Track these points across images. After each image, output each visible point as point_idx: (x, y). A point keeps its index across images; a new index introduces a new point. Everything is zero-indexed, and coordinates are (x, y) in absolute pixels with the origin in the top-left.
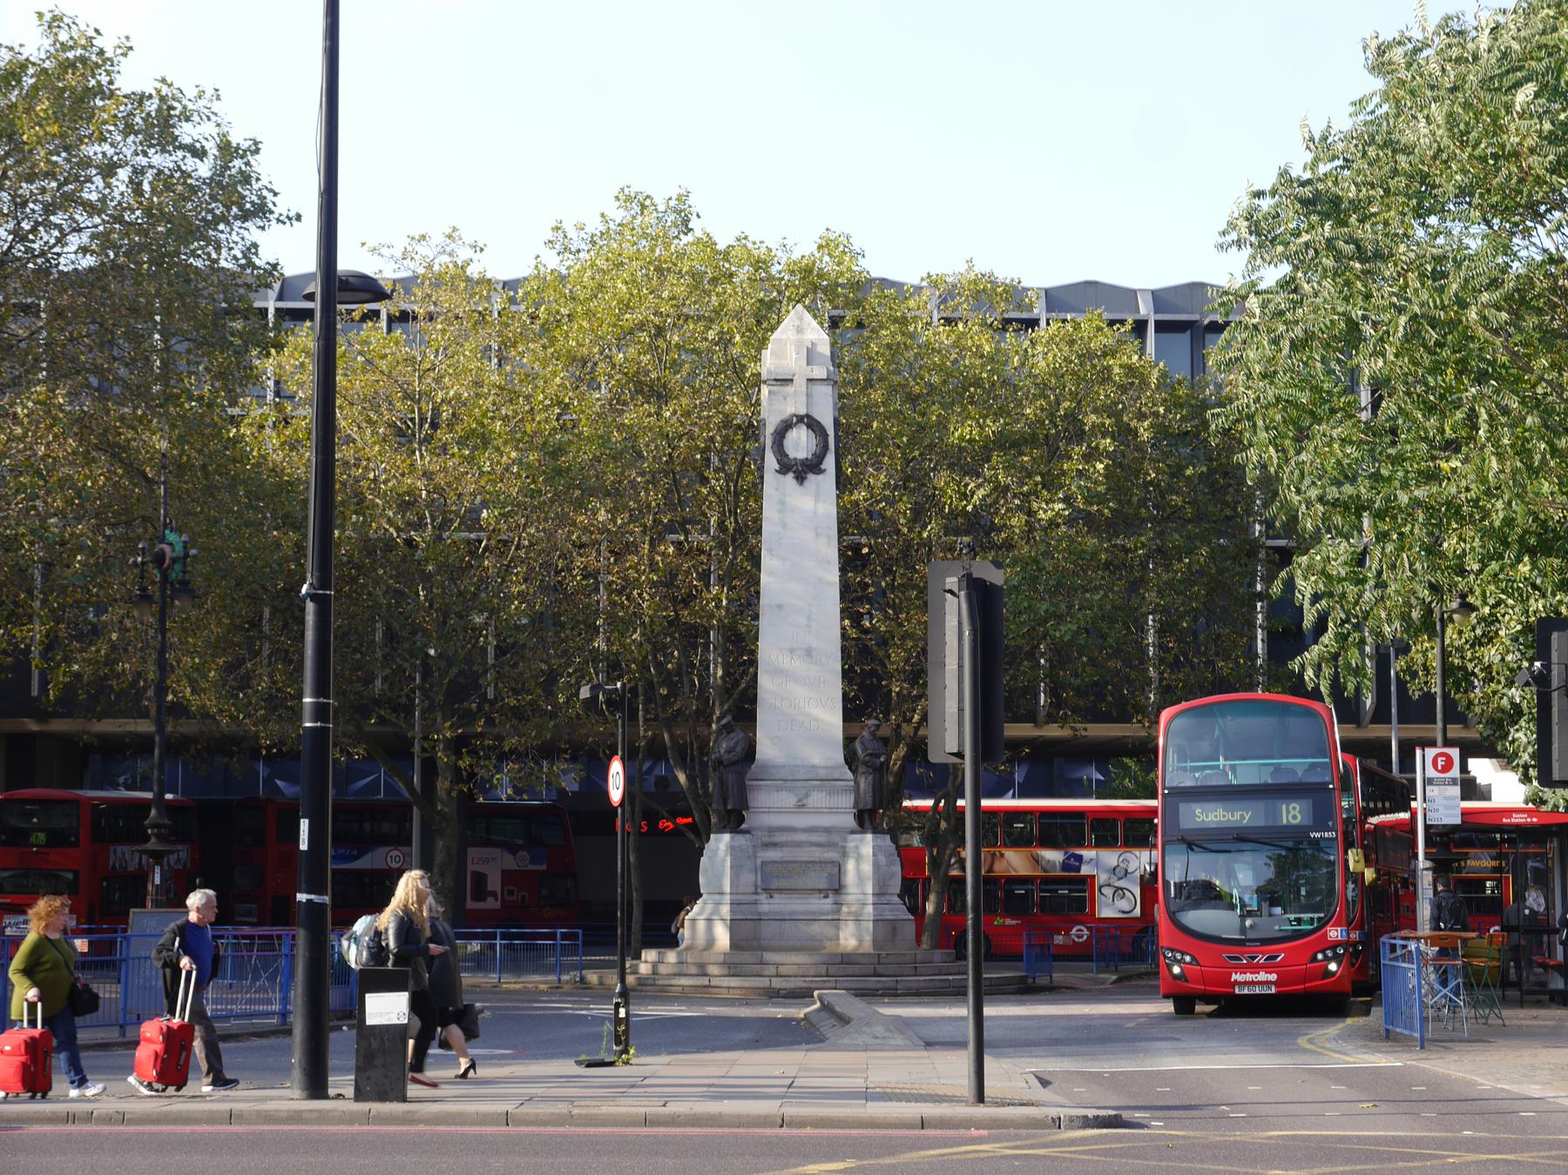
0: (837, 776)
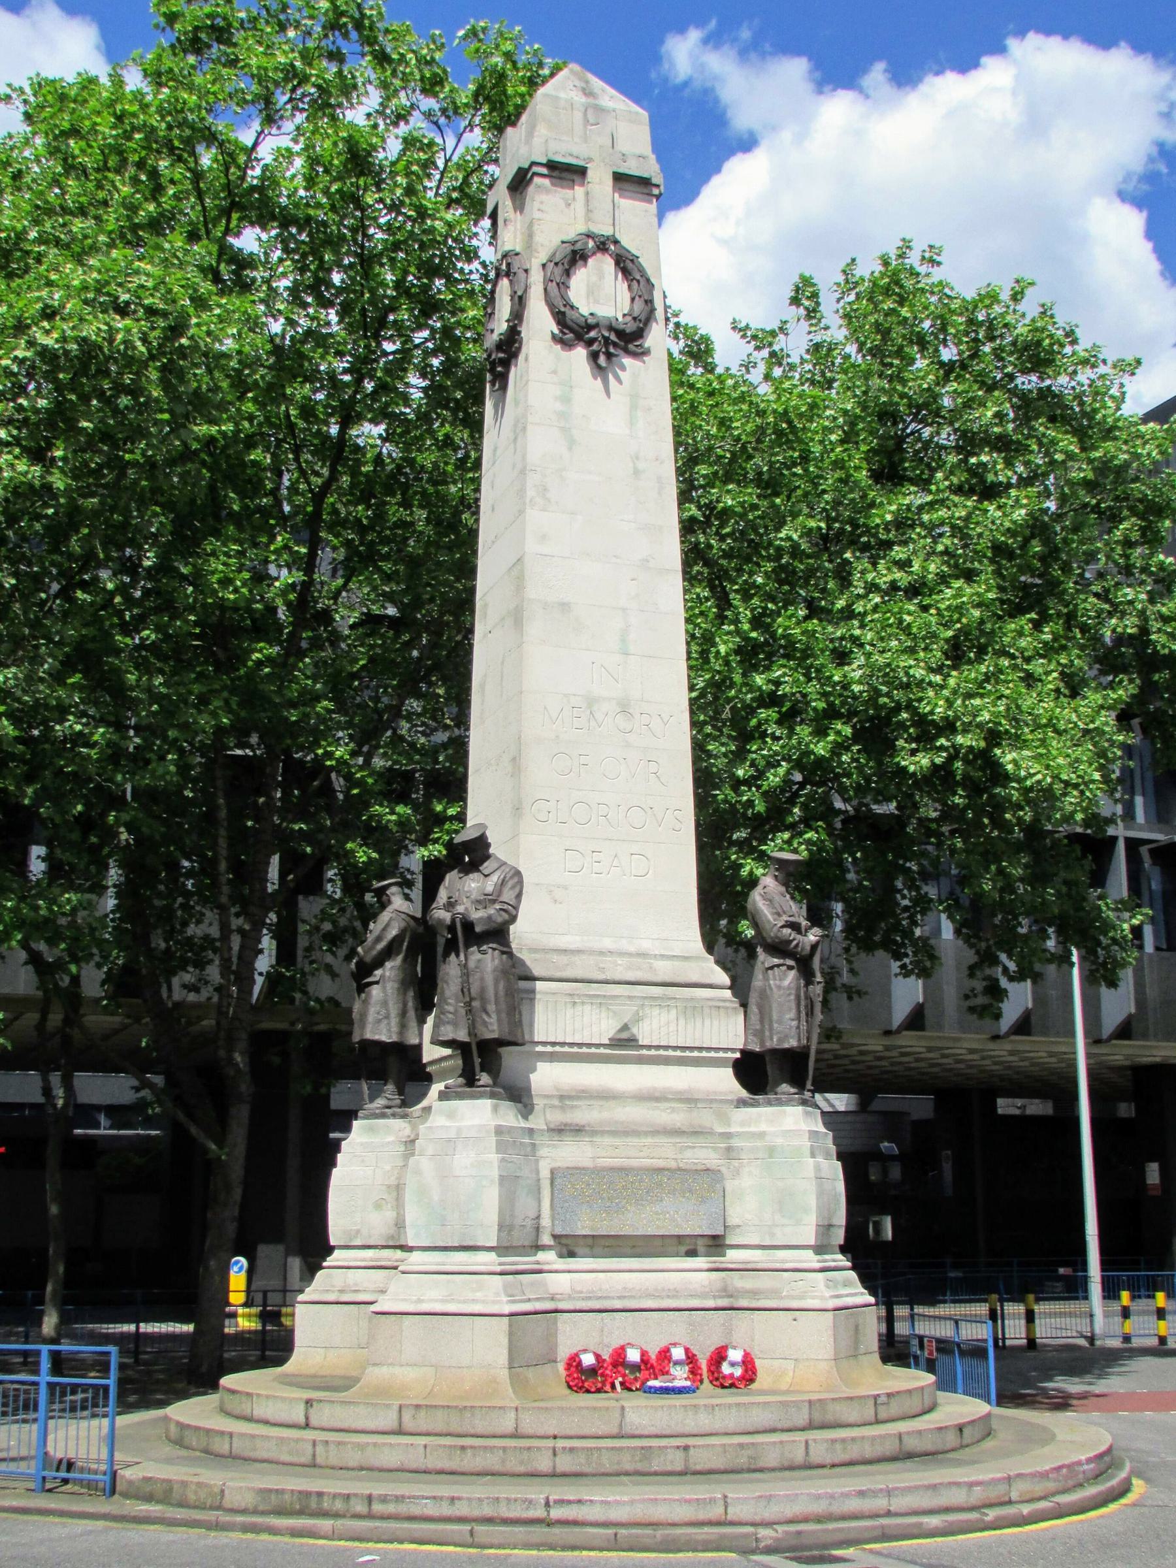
0: (695, 978)
